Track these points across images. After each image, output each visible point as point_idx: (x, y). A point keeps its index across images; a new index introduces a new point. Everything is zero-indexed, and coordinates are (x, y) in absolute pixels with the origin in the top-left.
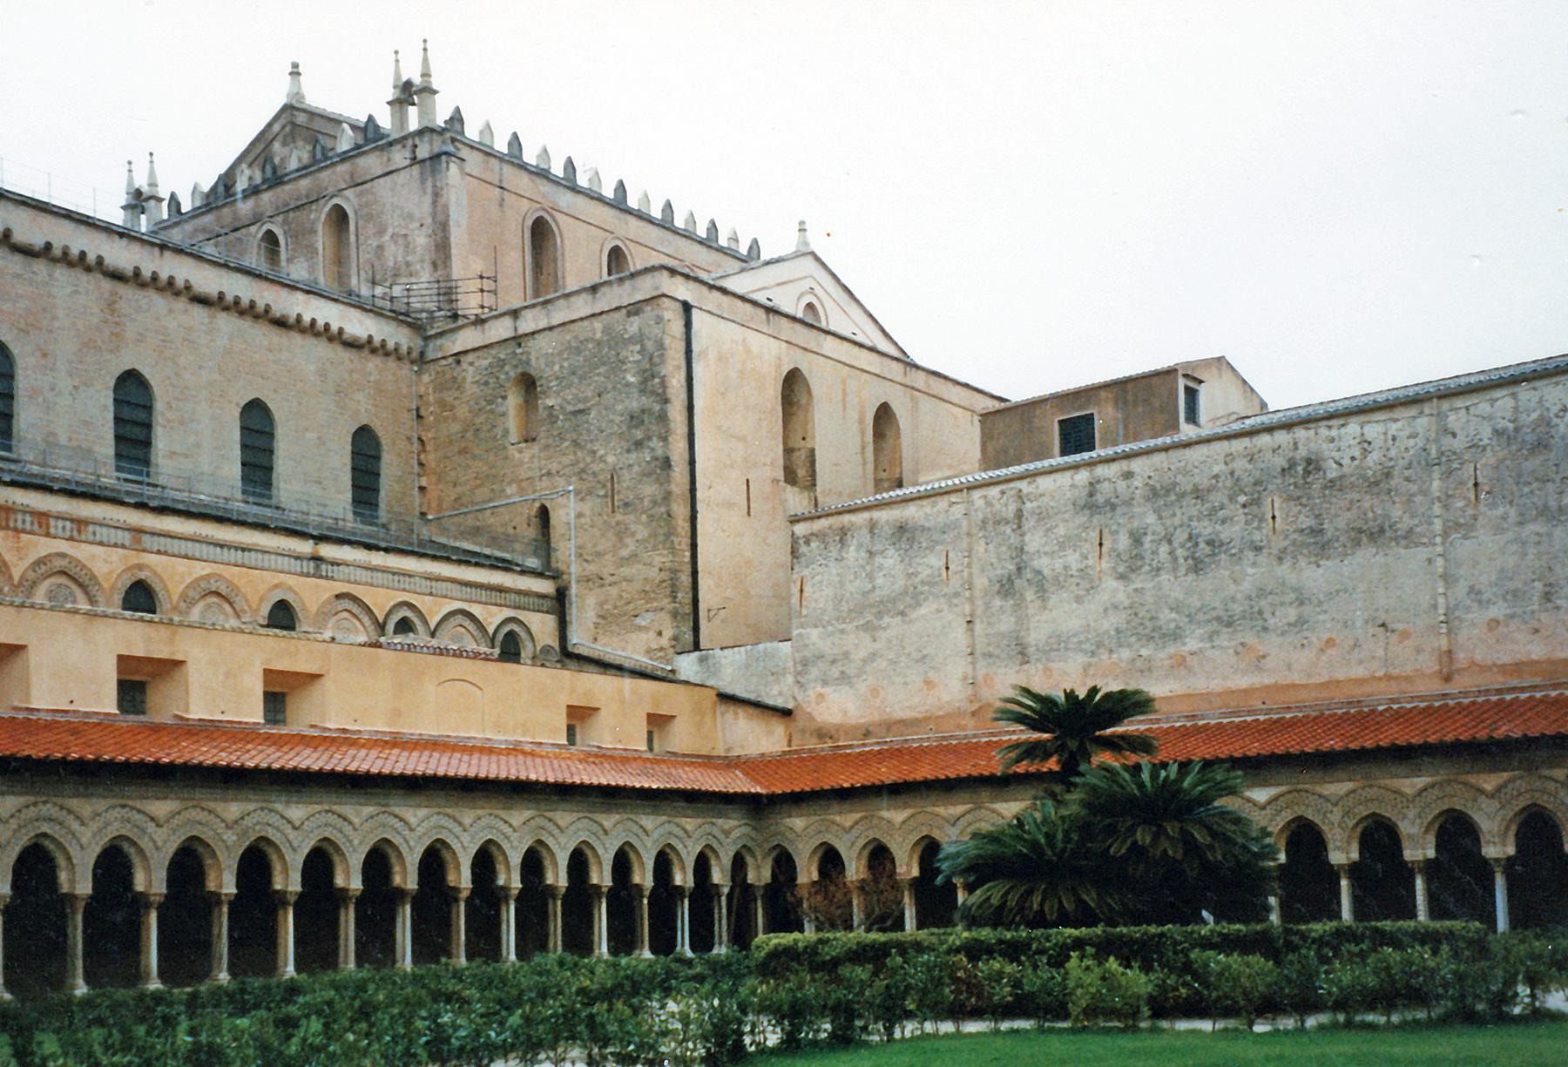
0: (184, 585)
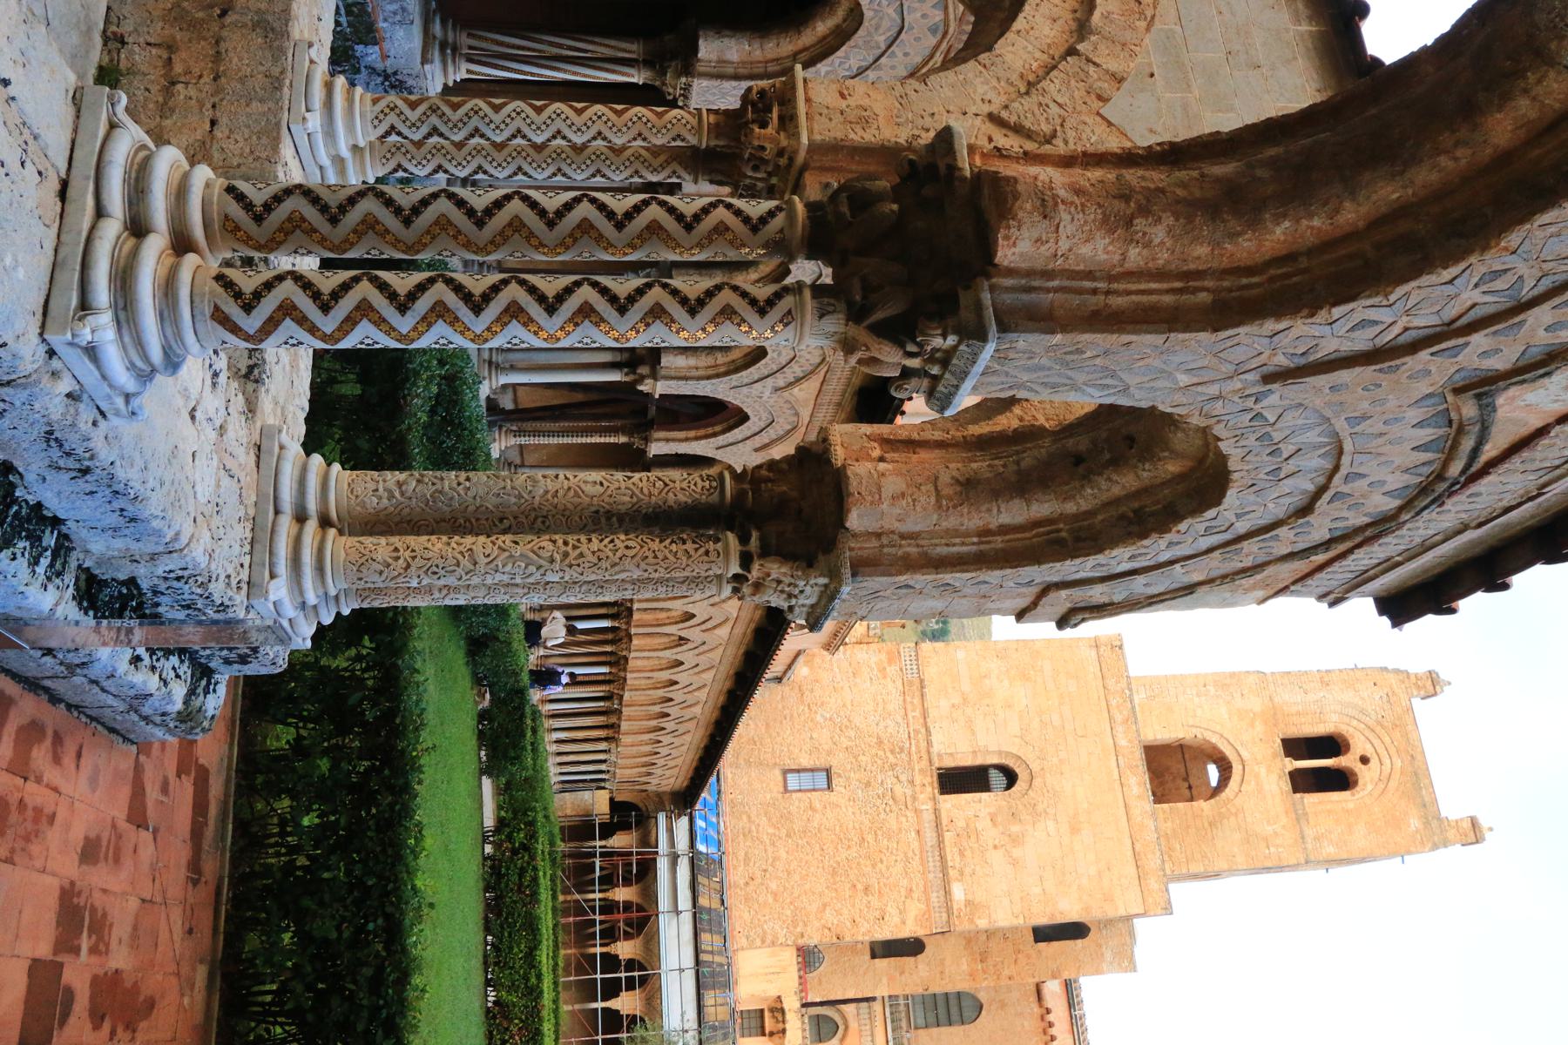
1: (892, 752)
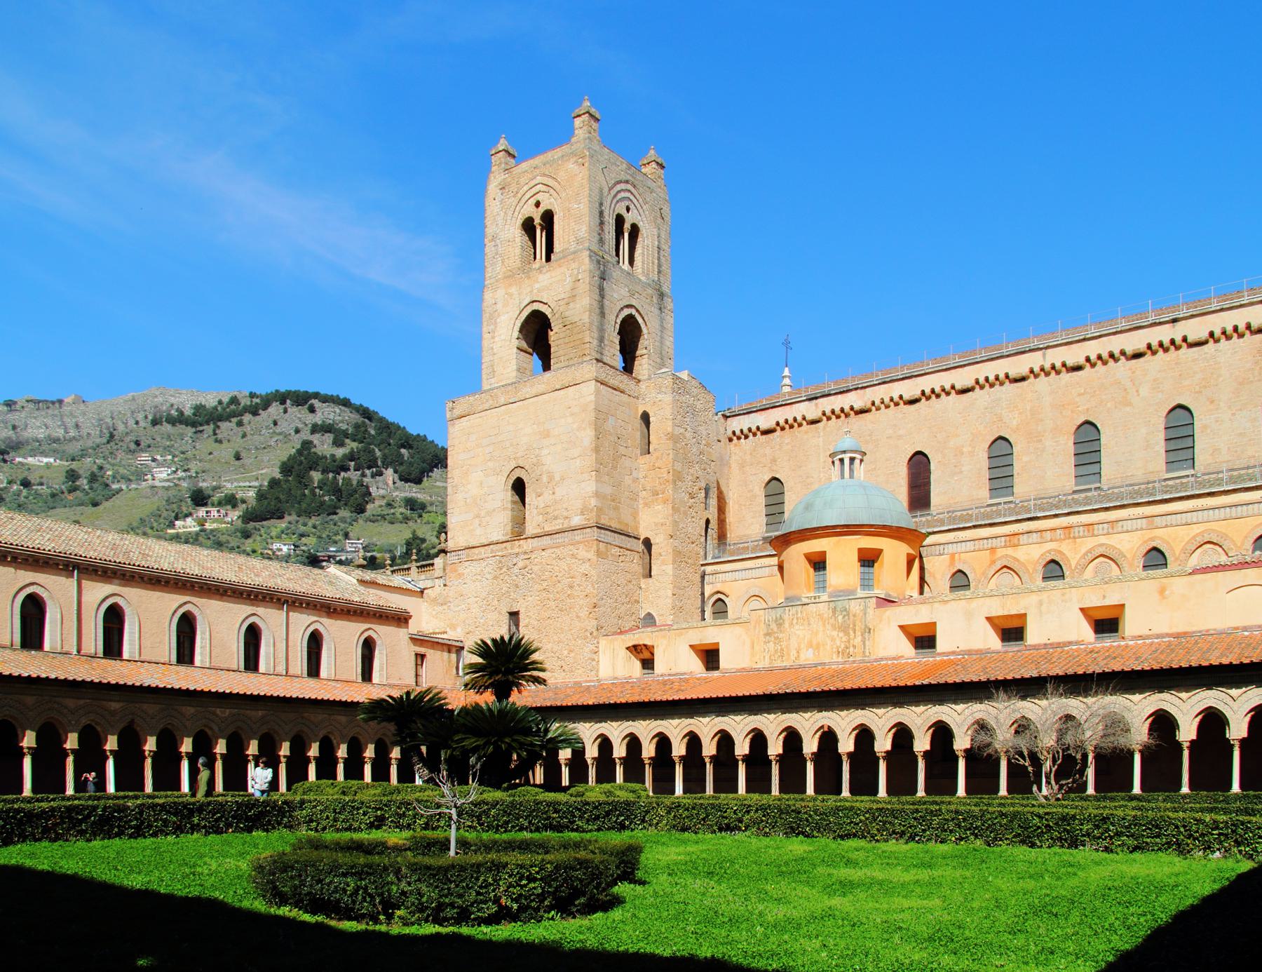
0: (1184, 543)
1: (501, 569)
